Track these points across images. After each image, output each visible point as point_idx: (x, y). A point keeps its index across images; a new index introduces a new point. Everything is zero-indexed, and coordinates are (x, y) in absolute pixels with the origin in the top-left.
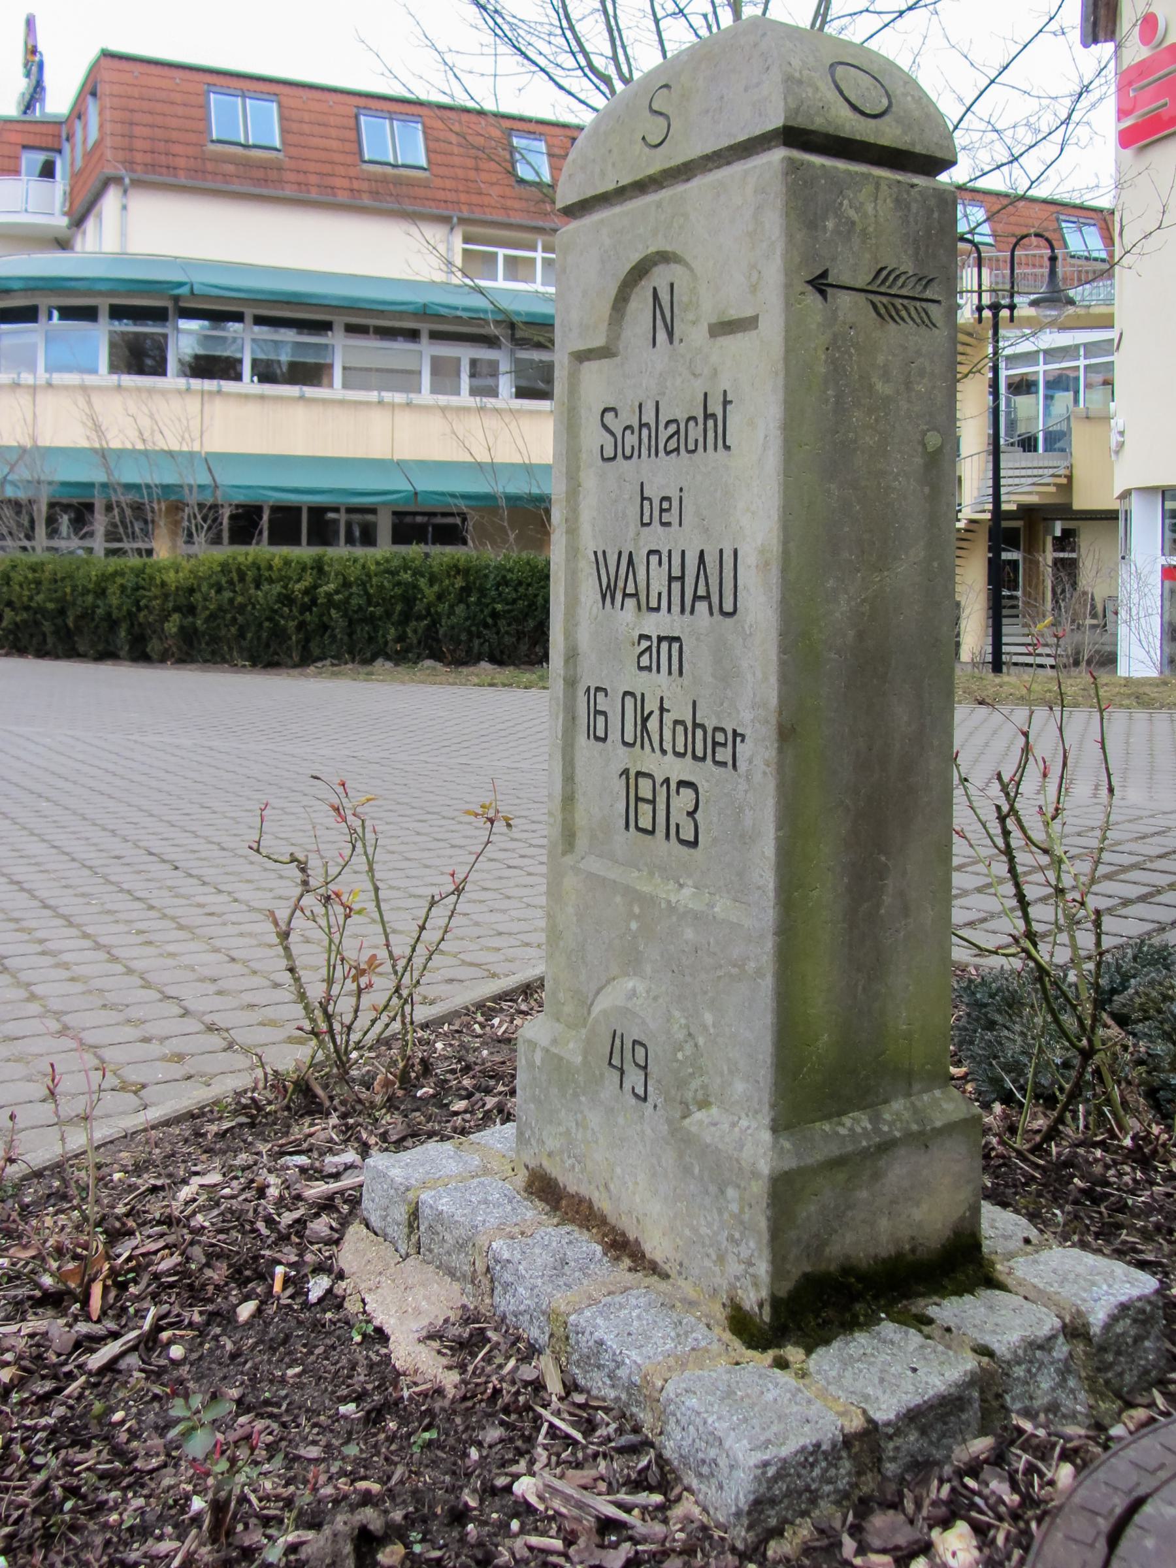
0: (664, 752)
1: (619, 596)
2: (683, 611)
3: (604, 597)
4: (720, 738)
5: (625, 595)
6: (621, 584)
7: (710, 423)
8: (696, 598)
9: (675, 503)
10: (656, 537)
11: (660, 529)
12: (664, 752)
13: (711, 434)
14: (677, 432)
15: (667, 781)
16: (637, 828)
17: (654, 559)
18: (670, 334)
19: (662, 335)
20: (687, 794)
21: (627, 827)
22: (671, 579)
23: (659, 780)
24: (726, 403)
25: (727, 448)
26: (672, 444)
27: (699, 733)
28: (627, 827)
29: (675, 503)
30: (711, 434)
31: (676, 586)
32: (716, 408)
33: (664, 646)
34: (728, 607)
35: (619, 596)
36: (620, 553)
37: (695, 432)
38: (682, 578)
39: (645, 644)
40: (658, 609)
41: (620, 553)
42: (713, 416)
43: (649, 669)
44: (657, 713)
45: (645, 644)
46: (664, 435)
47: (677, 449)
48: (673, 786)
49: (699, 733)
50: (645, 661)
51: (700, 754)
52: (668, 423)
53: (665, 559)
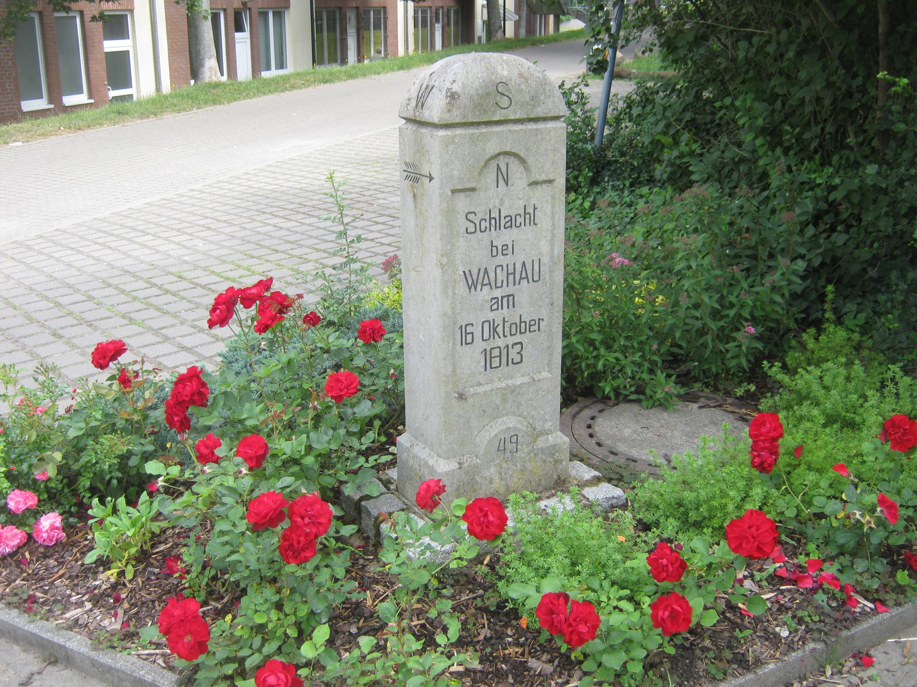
0: (505, 336)
2: (514, 284)
3: (470, 288)
5: (483, 285)
7: (527, 216)
8: (521, 278)
9: (510, 247)
10: (501, 260)
11: (502, 257)
12: (505, 336)
13: (527, 221)
16: (491, 368)
17: (499, 269)
18: (507, 184)
19: (501, 182)
24: (535, 209)
25: (535, 224)
26: (509, 224)
27: (523, 325)
29: (510, 247)
30: (527, 221)
32: (530, 210)
33: (505, 300)
35: (479, 287)
37: (519, 220)
38: (514, 273)
39: (494, 301)
40: (502, 287)
42: (529, 214)
45: (494, 301)
46: (503, 222)
48: (510, 347)
49: (523, 325)
51: (523, 330)
53: (505, 268)
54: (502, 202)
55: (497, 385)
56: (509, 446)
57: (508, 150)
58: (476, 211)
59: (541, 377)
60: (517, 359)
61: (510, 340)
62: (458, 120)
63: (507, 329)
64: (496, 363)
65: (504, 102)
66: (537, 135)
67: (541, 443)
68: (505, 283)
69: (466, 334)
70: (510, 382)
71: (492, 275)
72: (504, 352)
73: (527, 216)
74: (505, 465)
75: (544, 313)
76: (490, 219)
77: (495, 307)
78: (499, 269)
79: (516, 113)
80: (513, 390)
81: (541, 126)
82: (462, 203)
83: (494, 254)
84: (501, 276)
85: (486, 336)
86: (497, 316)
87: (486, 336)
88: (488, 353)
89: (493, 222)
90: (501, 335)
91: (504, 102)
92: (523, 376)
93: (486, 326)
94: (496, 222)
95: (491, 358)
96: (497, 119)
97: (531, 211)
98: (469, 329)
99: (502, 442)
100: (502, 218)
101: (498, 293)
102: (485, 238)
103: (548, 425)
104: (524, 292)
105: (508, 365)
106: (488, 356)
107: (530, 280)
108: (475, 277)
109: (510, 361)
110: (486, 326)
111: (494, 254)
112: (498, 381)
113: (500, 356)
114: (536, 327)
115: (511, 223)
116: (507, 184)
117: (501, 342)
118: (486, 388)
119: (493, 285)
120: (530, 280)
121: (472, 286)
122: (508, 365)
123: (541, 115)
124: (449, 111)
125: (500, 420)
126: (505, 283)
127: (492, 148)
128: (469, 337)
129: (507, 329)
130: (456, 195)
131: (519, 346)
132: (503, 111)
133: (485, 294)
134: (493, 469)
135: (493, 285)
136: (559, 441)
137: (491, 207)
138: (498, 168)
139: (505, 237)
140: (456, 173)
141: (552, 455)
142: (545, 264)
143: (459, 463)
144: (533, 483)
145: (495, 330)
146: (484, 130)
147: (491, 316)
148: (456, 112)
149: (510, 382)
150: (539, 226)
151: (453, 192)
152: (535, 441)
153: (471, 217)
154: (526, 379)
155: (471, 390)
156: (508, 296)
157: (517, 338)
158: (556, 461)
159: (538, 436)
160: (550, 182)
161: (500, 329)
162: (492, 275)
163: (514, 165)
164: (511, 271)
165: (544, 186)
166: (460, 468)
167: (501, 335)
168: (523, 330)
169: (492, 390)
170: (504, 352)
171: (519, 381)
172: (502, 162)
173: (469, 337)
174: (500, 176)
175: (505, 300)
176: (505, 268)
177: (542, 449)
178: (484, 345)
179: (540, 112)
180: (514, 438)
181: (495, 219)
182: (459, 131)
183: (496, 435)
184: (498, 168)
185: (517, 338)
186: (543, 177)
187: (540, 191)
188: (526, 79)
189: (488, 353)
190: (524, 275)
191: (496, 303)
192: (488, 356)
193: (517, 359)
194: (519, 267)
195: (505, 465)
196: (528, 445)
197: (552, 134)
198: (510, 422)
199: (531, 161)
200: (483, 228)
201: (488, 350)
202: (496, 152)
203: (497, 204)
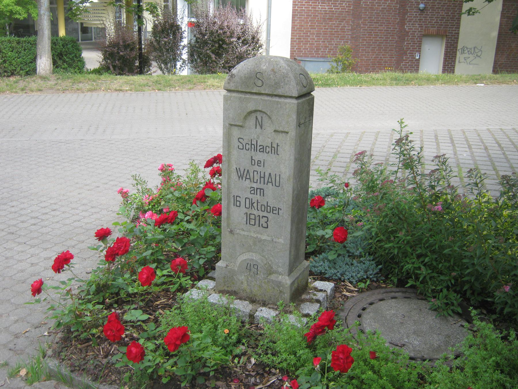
1: (244, 179)
2: (264, 184)
3: (239, 178)
4: (274, 209)
5: (246, 178)
6: (245, 175)
8: (268, 182)
9: (262, 163)
10: (256, 168)
13: (273, 151)
14: (263, 148)
15: (259, 216)
17: (255, 173)
18: (261, 128)
19: (258, 126)
20: (265, 219)
21: (247, 223)
22: (260, 177)
23: (256, 215)
24: (278, 146)
26: (262, 150)
27: (269, 208)
28: (247, 223)
29: (262, 163)
30: (273, 151)
31: (262, 179)
33: (258, 190)
34: (277, 185)
35: (244, 179)
36: (244, 170)
37: (268, 149)
38: (264, 178)
39: (252, 189)
40: (257, 182)
41: (244, 170)
42: (274, 147)
43: (254, 194)
44: (256, 203)
45: (252, 189)
46: (258, 148)
47: (263, 151)
49: (269, 208)
50: (253, 192)
51: (269, 210)
52: (260, 146)
53: (259, 173)
54: (258, 137)
55: (252, 234)
56: (253, 269)
57: (260, 109)
58: (244, 138)
59: (277, 240)
60: (265, 225)
61: (262, 214)
62: (233, 89)
63: (259, 207)
64: (252, 222)
65: (259, 83)
66: (278, 104)
67: (273, 277)
68: (259, 181)
69: (237, 201)
70: (259, 236)
71: (252, 175)
72: (257, 219)
73: (273, 149)
74: (250, 278)
75: (281, 206)
76: (251, 144)
77: (253, 192)
78: (255, 173)
79: (265, 90)
80: (260, 241)
81: (282, 100)
82: (236, 133)
83: (253, 164)
84: (257, 177)
85: (247, 206)
86: (255, 198)
87: (247, 206)
88: (248, 215)
89: (253, 146)
90: (256, 208)
91: (259, 83)
92: (268, 236)
93: (247, 200)
94: (254, 146)
95: (250, 218)
96: (254, 91)
97: (276, 146)
98: (238, 199)
99: (249, 265)
100: (258, 146)
101: (255, 185)
102: (248, 154)
103: (280, 270)
104: (269, 189)
105: (259, 226)
106: (248, 217)
107: (274, 185)
108: (242, 173)
109: (261, 225)
110: (247, 200)
111: (253, 164)
112: (254, 232)
113: (255, 219)
114: (277, 212)
115: (263, 149)
116: (261, 128)
117: (255, 212)
118: (246, 233)
119: (252, 180)
120: (274, 185)
121: (241, 177)
122: (259, 226)
123: (281, 94)
124: (229, 83)
125: (251, 254)
126: (259, 181)
127: (251, 107)
128: (238, 203)
129: (259, 207)
130: (233, 127)
131: (266, 218)
132: (258, 88)
133: (247, 183)
134: (243, 277)
135: (252, 180)
136: (284, 281)
137: (252, 138)
138: (257, 118)
139: (259, 156)
140: (231, 115)
141: (279, 287)
142: (283, 178)
143: (227, 265)
144: (266, 297)
145: (252, 204)
146: (248, 96)
147: (251, 196)
148: (232, 84)
149: (259, 236)
150: (280, 156)
151: (231, 125)
152: (270, 274)
153: (240, 140)
154: (269, 239)
155: (238, 231)
156: (261, 189)
157: (265, 214)
158: (281, 292)
159: (273, 273)
160: (287, 133)
161: (255, 205)
162: (252, 175)
163: (266, 119)
164: (262, 175)
165: (284, 134)
166: (226, 267)
167: (256, 209)
168: (269, 210)
169: (248, 236)
170: (257, 219)
171: (264, 237)
172: (259, 115)
173: (238, 203)
174: (257, 123)
175: (258, 190)
176: (259, 173)
177: (273, 281)
178: (246, 210)
179: (280, 92)
180: (256, 266)
181: (254, 145)
182: (234, 94)
183: (245, 260)
184: (257, 118)
185: (265, 214)
186: (281, 129)
187: (281, 136)
188: (275, 72)
189: (248, 215)
190: (270, 180)
191: (254, 191)
192: (248, 217)
193: (265, 225)
194: (267, 175)
195: (250, 278)
196: (264, 274)
197: (287, 106)
198: (255, 257)
199: (274, 118)
200: (247, 148)
201: (248, 213)
202: (254, 109)
203: (255, 137)
